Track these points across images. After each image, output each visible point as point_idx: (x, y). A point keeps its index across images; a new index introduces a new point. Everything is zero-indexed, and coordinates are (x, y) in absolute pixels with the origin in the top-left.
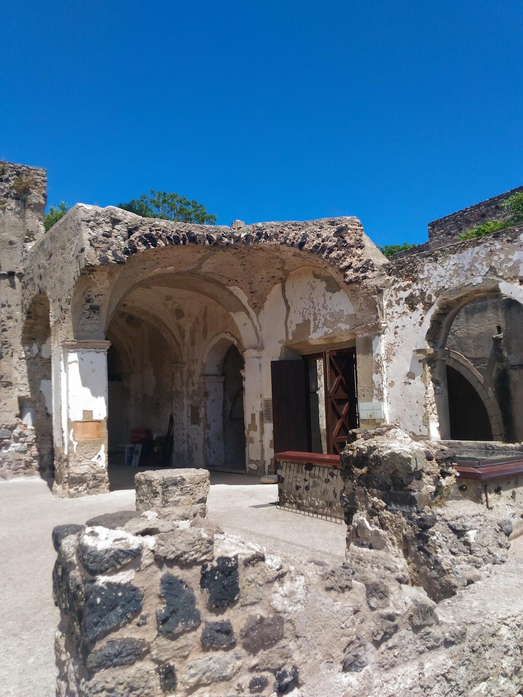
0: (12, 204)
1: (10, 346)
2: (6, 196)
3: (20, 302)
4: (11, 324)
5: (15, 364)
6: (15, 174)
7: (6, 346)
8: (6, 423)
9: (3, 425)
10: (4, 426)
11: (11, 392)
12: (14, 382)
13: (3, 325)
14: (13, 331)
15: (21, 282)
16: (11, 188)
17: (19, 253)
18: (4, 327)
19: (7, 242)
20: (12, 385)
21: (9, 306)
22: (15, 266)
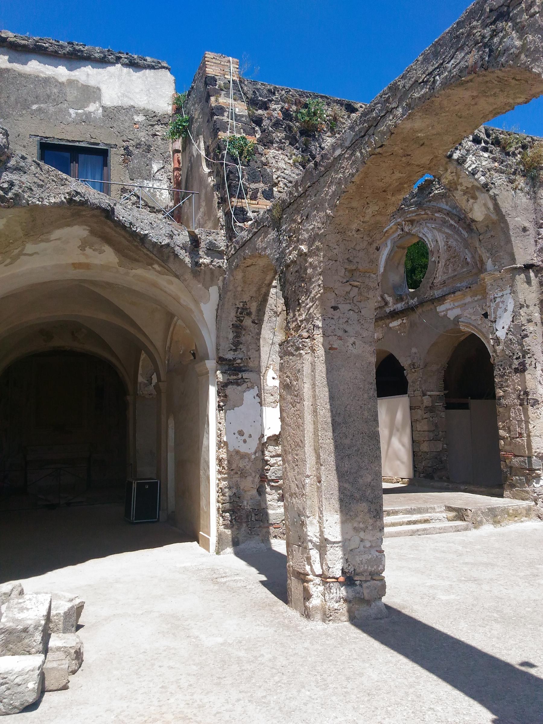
0: (521, 182)
1: (533, 355)
2: (514, 173)
3: (538, 302)
4: (532, 329)
5: (539, 378)
6: (519, 147)
7: (529, 355)
8: (538, 450)
9: (536, 452)
10: (536, 454)
11: (538, 412)
12: (539, 399)
13: (523, 330)
14: (534, 337)
15: (536, 276)
16: (518, 164)
17: (532, 242)
18: (525, 332)
19: (521, 229)
20: (539, 404)
21: (528, 306)
22: (529, 258)
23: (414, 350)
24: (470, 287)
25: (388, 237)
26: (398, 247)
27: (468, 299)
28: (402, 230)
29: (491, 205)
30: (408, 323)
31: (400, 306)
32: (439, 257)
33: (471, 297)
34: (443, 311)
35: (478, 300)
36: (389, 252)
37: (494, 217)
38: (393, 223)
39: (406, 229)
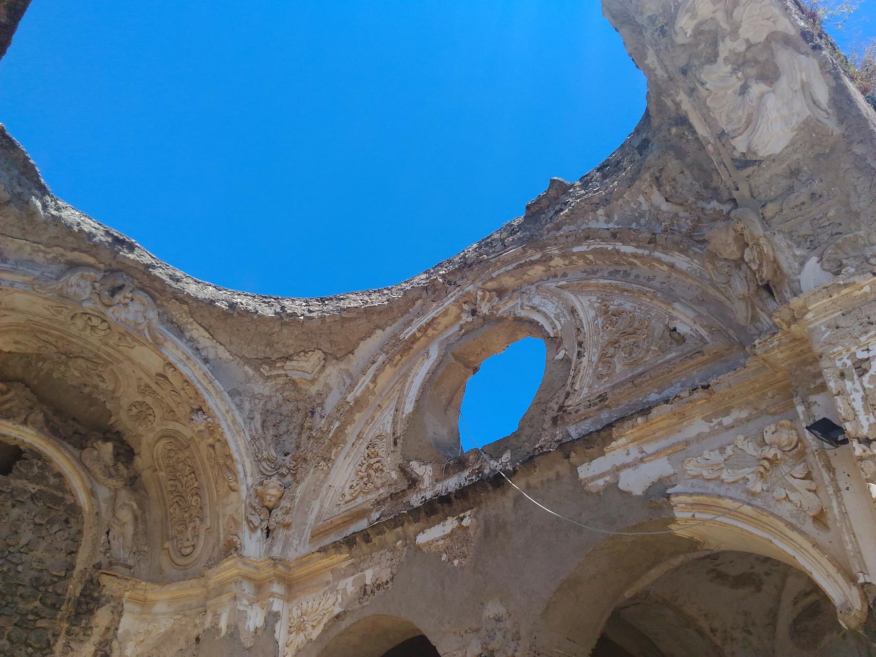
23: (493, 609)
24: (706, 387)
25: (432, 339)
26: (457, 358)
27: (697, 427)
28: (474, 312)
29: (822, 94)
30: (478, 527)
31: (452, 483)
32: (580, 344)
33: (708, 419)
34: (602, 475)
35: (739, 422)
36: (434, 367)
37: (832, 125)
38: (453, 299)
39: (484, 309)
